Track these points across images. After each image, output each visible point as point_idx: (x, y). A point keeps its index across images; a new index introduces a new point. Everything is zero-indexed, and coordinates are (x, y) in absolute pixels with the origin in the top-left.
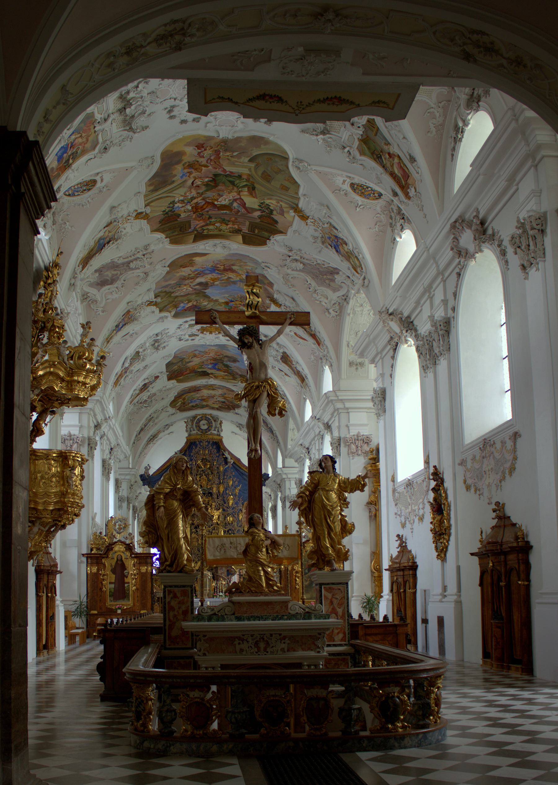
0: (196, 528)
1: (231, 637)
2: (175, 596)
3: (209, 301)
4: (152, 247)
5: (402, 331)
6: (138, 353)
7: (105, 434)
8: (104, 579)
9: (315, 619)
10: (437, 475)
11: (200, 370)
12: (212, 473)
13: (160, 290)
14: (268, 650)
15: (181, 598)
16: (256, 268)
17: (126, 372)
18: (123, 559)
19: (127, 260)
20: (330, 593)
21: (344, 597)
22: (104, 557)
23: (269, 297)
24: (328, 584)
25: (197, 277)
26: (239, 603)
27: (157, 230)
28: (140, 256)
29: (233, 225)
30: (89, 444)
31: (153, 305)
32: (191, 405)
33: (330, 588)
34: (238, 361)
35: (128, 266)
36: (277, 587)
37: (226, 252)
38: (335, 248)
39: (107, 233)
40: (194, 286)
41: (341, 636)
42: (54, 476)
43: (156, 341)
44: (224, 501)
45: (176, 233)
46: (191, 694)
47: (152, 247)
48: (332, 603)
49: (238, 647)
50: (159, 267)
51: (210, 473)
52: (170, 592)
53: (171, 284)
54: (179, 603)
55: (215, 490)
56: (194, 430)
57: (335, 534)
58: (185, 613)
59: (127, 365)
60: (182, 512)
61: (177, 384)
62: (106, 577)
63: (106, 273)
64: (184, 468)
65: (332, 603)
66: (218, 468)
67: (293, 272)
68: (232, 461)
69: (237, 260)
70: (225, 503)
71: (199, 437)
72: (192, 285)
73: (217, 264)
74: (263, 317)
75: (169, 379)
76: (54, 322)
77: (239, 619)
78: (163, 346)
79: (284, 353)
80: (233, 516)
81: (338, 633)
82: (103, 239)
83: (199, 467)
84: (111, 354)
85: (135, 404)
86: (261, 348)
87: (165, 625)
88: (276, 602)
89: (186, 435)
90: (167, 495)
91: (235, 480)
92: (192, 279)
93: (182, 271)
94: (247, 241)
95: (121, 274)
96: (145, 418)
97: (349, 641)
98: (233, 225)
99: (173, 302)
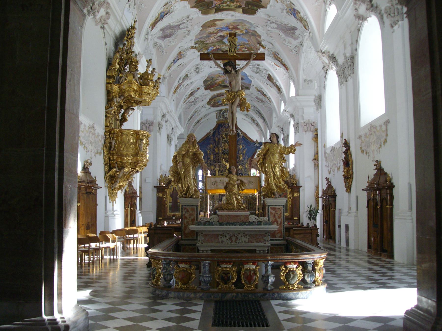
1: (217, 234)
2: (188, 211)
3: (226, 46)
4: (191, 17)
5: (329, 62)
6: (187, 75)
7: (168, 120)
8: (166, 200)
9: (264, 225)
10: (346, 144)
11: (223, 84)
13: (198, 40)
14: (237, 241)
15: (191, 212)
16: (251, 27)
17: (180, 86)
18: (177, 189)
19: (177, 24)
20: (274, 210)
21: (282, 213)
22: (166, 188)
23: (259, 43)
24: (273, 206)
25: (218, 33)
26: (221, 215)
27: (193, 7)
28: (185, 22)
29: (237, 3)
30: (158, 126)
31: (194, 48)
32: (219, 103)
33: (274, 208)
34: (244, 79)
35: (179, 27)
36: (243, 207)
37: (234, 18)
38: (294, 15)
39: (165, 9)
40: (218, 37)
41: (279, 235)
42: (132, 144)
43: (197, 68)
45: (205, 8)
46: (181, 266)
47: (191, 17)
48: (275, 216)
49: (220, 240)
50: (196, 27)
52: (185, 209)
53: (203, 37)
54: (190, 215)
56: (221, 118)
57: (278, 178)
58: (193, 220)
59: (181, 82)
60: (193, 164)
61: (211, 92)
62: (167, 199)
63: (166, 31)
64: (193, 141)
65: (275, 216)
67: (272, 29)
68: (242, 135)
69: (240, 23)
71: (223, 121)
72: (215, 37)
73: (229, 25)
74: (238, 56)
75: (206, 89)
76: (132, 60)
77: (221, 224)
78: (201, 71)
79: (269, 75)
80: (242, 166)
81: (278, 233)
82: (163, 13)
83: (223, 138)
84: (172, 76)
85: (186, 104)
86: (236, 73)
87: (182, 227)
88: (242, 215)
89: (217, 120)
90: (183, 156)
91: (243, 145)
92: (215, 33)
93: (209, 30)
94: (245, 12)
95: (175, 32)
96: (193, 111)
97: (284, 237)
98: (237, 3)
99: (205, 46)
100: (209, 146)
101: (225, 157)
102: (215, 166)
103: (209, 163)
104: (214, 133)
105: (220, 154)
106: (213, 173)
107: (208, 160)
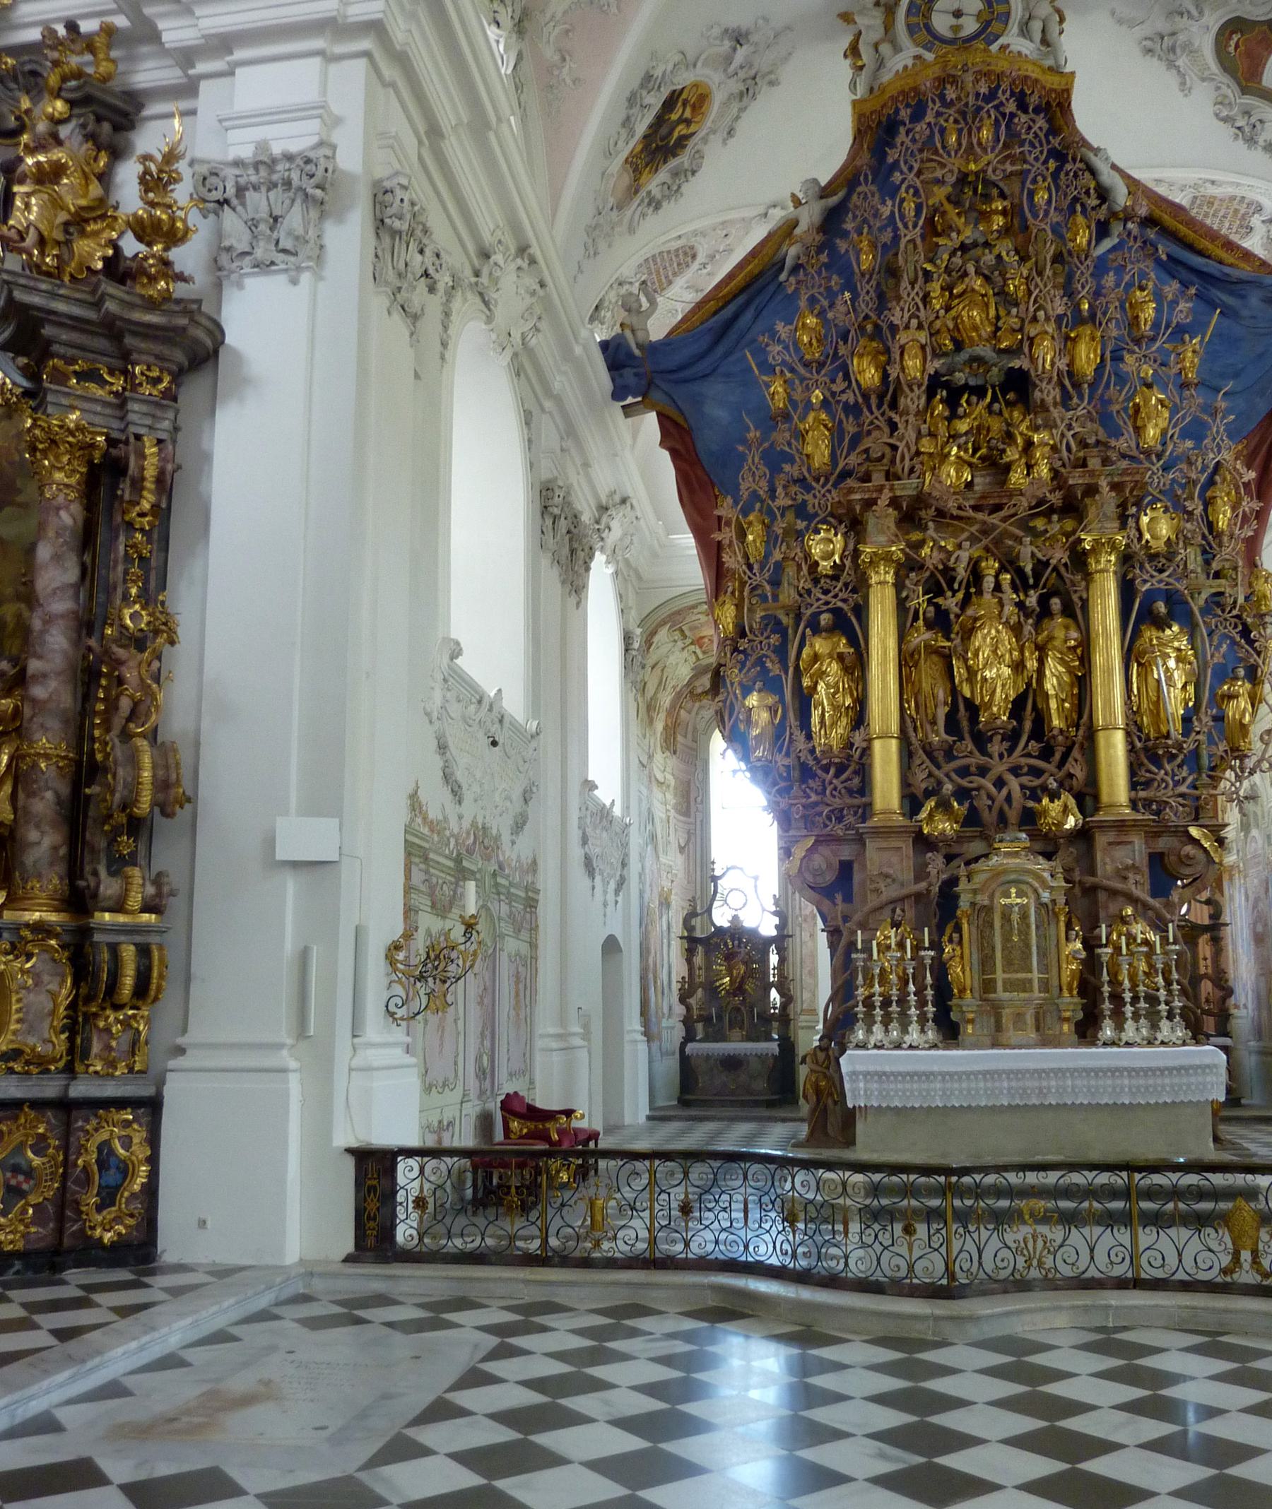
0: (934, 589)
12: (1024, 259)
44: (1105, 419)
55: (1047, 354)
56: (897, 49)
80: (1177, 506)
100: (782, 329)
101: (963, 426)
102: (854, 526)
103: (782, 501)
104: (831, 222)
106: (836, 612)
107: (775, 469)
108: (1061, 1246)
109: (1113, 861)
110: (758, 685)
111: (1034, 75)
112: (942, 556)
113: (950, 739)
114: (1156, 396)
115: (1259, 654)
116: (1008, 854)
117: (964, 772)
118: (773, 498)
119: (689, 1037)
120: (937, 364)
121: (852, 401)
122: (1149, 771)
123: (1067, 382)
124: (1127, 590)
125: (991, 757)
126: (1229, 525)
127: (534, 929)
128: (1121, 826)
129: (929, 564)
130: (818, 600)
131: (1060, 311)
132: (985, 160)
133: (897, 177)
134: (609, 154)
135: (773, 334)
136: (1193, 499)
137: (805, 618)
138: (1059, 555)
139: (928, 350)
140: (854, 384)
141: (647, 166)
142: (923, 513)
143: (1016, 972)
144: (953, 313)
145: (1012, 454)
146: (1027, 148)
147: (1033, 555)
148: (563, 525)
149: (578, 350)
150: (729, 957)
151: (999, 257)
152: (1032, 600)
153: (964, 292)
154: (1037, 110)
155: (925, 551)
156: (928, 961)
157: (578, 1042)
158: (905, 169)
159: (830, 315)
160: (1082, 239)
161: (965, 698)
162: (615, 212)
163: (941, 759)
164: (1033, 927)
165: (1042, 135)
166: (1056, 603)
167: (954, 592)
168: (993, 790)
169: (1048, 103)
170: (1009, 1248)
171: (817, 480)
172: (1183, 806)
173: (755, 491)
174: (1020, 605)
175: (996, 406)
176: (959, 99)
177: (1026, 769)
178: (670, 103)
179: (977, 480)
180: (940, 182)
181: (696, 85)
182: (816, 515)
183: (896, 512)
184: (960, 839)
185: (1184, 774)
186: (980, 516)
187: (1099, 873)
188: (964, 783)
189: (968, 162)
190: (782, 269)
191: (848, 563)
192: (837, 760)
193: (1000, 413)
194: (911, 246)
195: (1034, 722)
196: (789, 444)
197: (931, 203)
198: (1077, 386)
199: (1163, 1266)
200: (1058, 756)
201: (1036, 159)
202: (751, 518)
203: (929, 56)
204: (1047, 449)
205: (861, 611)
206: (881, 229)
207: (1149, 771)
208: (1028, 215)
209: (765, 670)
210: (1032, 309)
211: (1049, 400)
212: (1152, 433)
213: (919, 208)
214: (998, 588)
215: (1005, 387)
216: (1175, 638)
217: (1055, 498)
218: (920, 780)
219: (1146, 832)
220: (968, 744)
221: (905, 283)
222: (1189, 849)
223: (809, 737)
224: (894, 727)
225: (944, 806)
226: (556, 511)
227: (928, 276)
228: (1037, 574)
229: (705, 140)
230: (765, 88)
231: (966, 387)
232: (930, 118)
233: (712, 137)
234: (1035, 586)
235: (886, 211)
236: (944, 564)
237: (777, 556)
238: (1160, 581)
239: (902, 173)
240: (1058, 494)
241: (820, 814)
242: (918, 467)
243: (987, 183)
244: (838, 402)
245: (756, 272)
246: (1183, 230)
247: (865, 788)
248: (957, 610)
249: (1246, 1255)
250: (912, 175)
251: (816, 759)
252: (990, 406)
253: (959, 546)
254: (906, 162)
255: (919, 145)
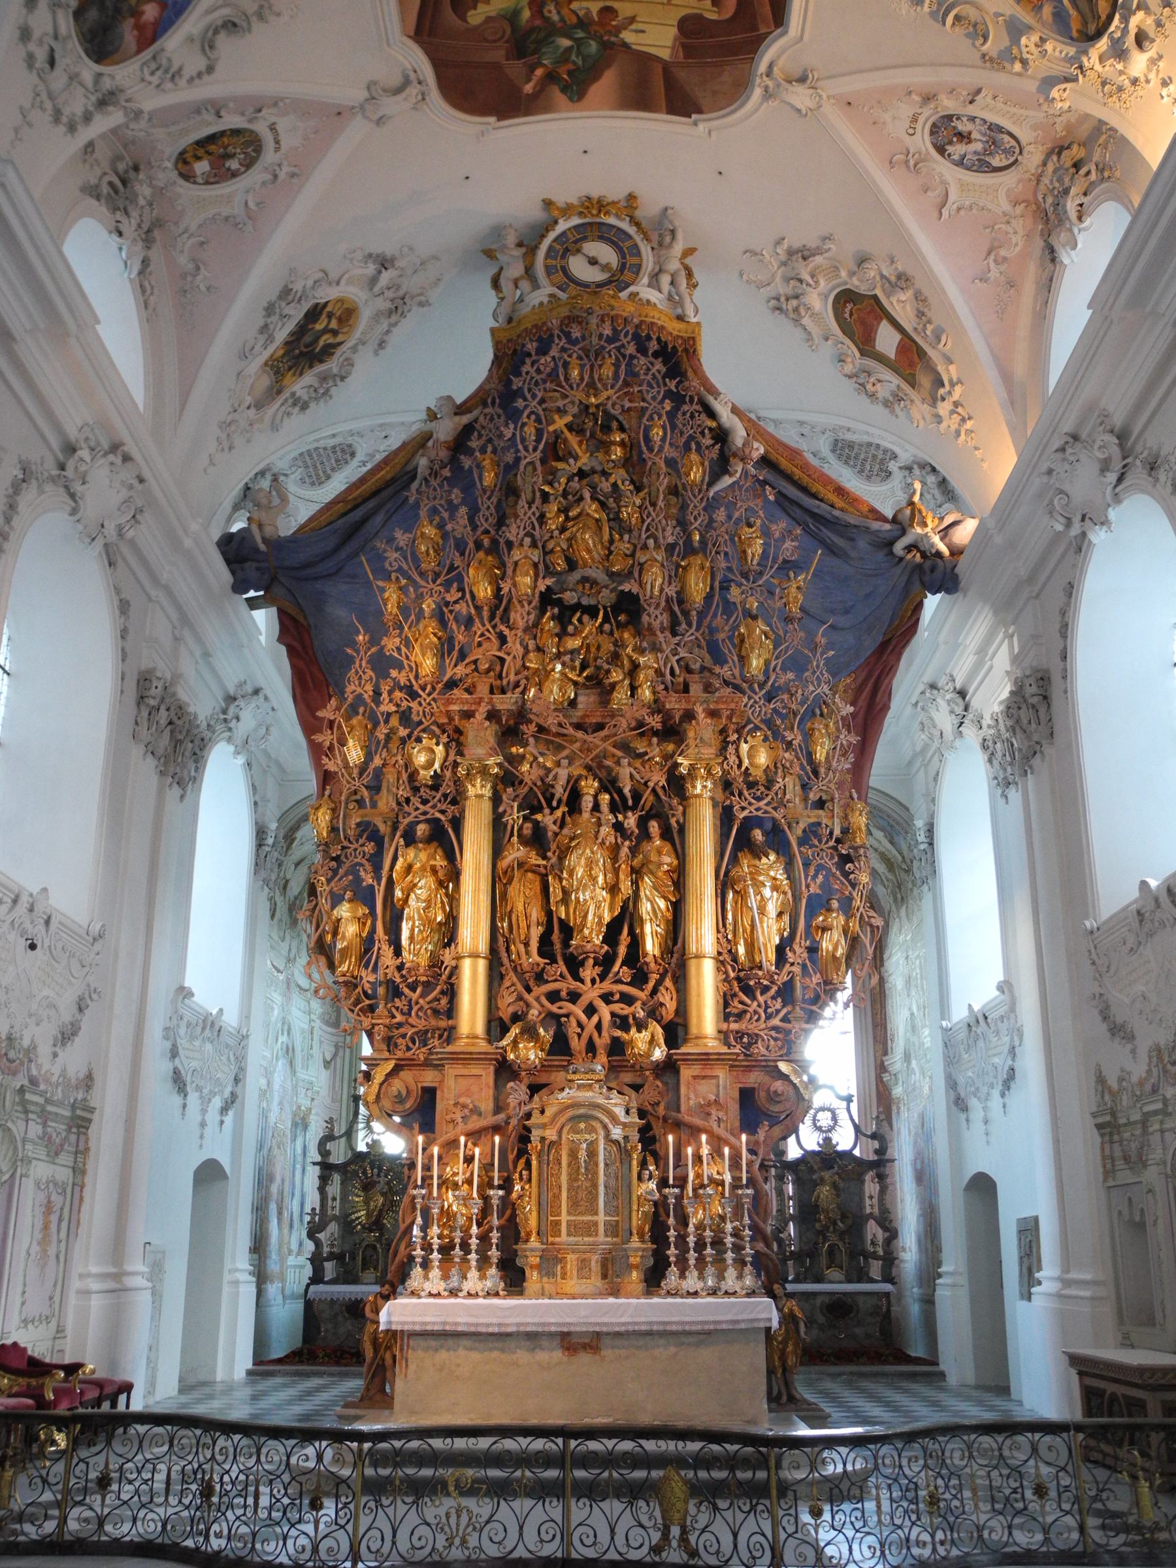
0: (531, 806)
12: (638, 489)
51: (626, 487)
55: (655, 581)
56: (536, 286)
66: (671, 463)
70: (719, 659)
80: (774, 735)
100: (402, 538)
101: (573, 643)
105: (520, 616)
106: (435, 824)
108: (488, 1522)
109: (696, 1096)
110: (348, 895)
111: (660, 323)
112: (542, 772)
113: (542, 961)
114: (761, 626)
115: (853, 885)
116: (580, 1087)
117: (553, 997)
118: (378, 703)
119: (317, 1278)
120: (549, 582)
121: (464, 611)
122: (742, 1002)
123: (676, 609)
124: (725, 817)
125: (582, 981)
126: (827, 758)
127: (82, 1152)
128: (706, 1059)
129: (527, 779)
130: (417, 809)
131: (670, 540)
132: (605, 394)
133: (520, 403)
134: (244, 356)
135: (391, 540)
136: (792, 729)
137: (401, 827)
138: (658, 779)
139: (541, 567)
140: (468, 596)
141: (290, 369)
142: (524, 728)
143: (581, 1214)
144: (568, 534)
145: (616, 676)
146: (644, 388)
147: (631, 776)
148: (163, 716)
149: (188, 543)
150: (367, 1187)
151: (615, 485)
152: (631, 821)
153: (580, 514)
154: (656, 355)
155: (525, 767)
156: (495, 1202)
157: (139, 1281)
158: (528, 396)
159: (449, 527)
160: (696, 475)
161: (560, 919)
162: (253, 411)
163: (531, 983)
164: (602, 1165)
165: (659, 377)
166: (654, 827)
167: (553, 810)
168: (583, 1017)
169: (674, 347)
170: (428, 1525)
171: (424, 689)
172: (776, 1039)
173: (360, 695)
174: (618, 827)
175: (607, 627)
176: (584, 338)
177: (617, 997)
178: (314, 313)
179: (581, 699)
180: (561, 411)
181: (341, 301)
182: (420, 723)
183: (495, 727)
184: (545, 1067)
185: (778, 1006)
186: (580, 734)
187: (683, 1108)
188: (554, 1008)
189: (588, 396)
190: (414, 478)
191: (448, 774)
192: (424, 979)
193: (611, 633)
194: (530, 468)
195: (628, 947)
196: (399, 649)
197: (551, 429)
198: (686, 614)
199: (594, 1544)
200: (651, 984)
201: (654, 398)
202: (354, 721)
203: (563, 296)
204: (651, 672)
205: (457, 823)
206: (505, 449)
207: (742, 1002)
208: (644, 448)
209: (358, 880)
210: (644, 536)
211: (656, 624)
212: (756, 663)
213: (539, 433)
214: (596, 807)
215: (617, 608)
216: (770, 867)
217: (655, 722)
218: (507, 1004)
219: (732, 1066)
220: (562, 967)
221: (522, 503)
222: (778, 1085)
223: (398, 952)
224: (483, 946)
225: (530, 1032)
226: (152, 702)
227: (545, 497)
228: (637, 796)
229: (354, 349)
230: (415, 309)
231: (577, 606)
232: (554, 352)
233: (360, 347)
234: (633, 809)
235: (508, 433)
236: (542, 780)
237: (377, 762)
238: (758, 809)
239: (525, 399)
240: (658, 718)
241: (404, 1036)
242: (523, 682)
243: (608, 416)
244: (451, 612)
245: (389, 477)
246: (797, 474)
247: (451, 1012)
248: (555, 828)
249: (675, 1531)
250: (534, 403)
251: (402, 976)
252: (602, 625)
253: (558, 764)
254: (530, 390)
255: (543, 376)
